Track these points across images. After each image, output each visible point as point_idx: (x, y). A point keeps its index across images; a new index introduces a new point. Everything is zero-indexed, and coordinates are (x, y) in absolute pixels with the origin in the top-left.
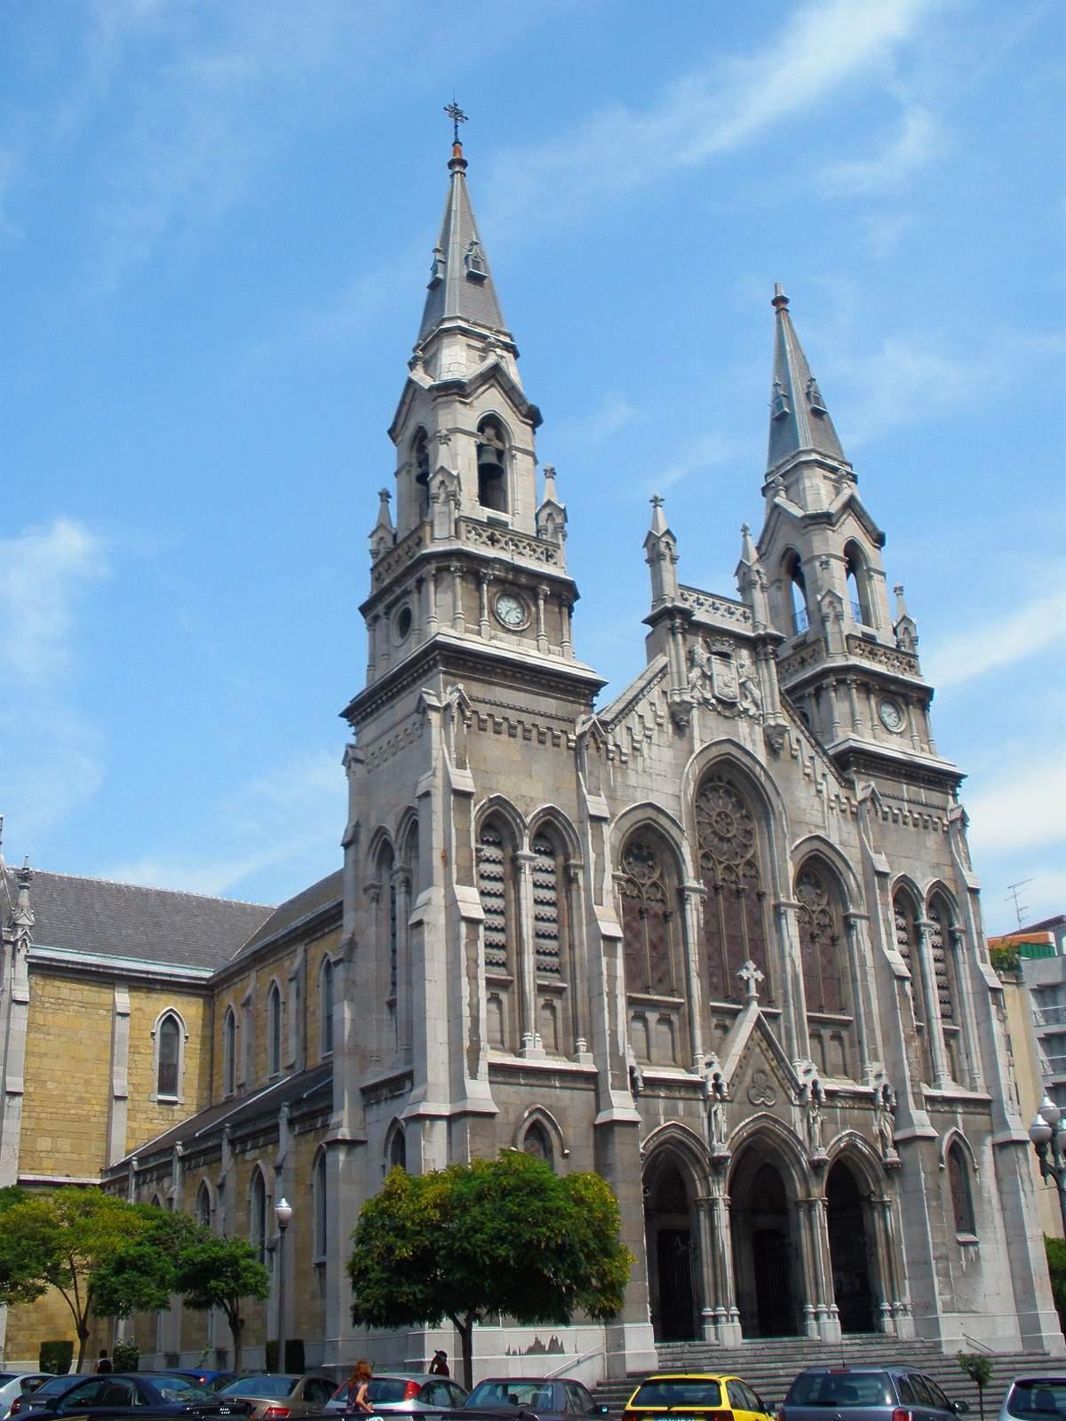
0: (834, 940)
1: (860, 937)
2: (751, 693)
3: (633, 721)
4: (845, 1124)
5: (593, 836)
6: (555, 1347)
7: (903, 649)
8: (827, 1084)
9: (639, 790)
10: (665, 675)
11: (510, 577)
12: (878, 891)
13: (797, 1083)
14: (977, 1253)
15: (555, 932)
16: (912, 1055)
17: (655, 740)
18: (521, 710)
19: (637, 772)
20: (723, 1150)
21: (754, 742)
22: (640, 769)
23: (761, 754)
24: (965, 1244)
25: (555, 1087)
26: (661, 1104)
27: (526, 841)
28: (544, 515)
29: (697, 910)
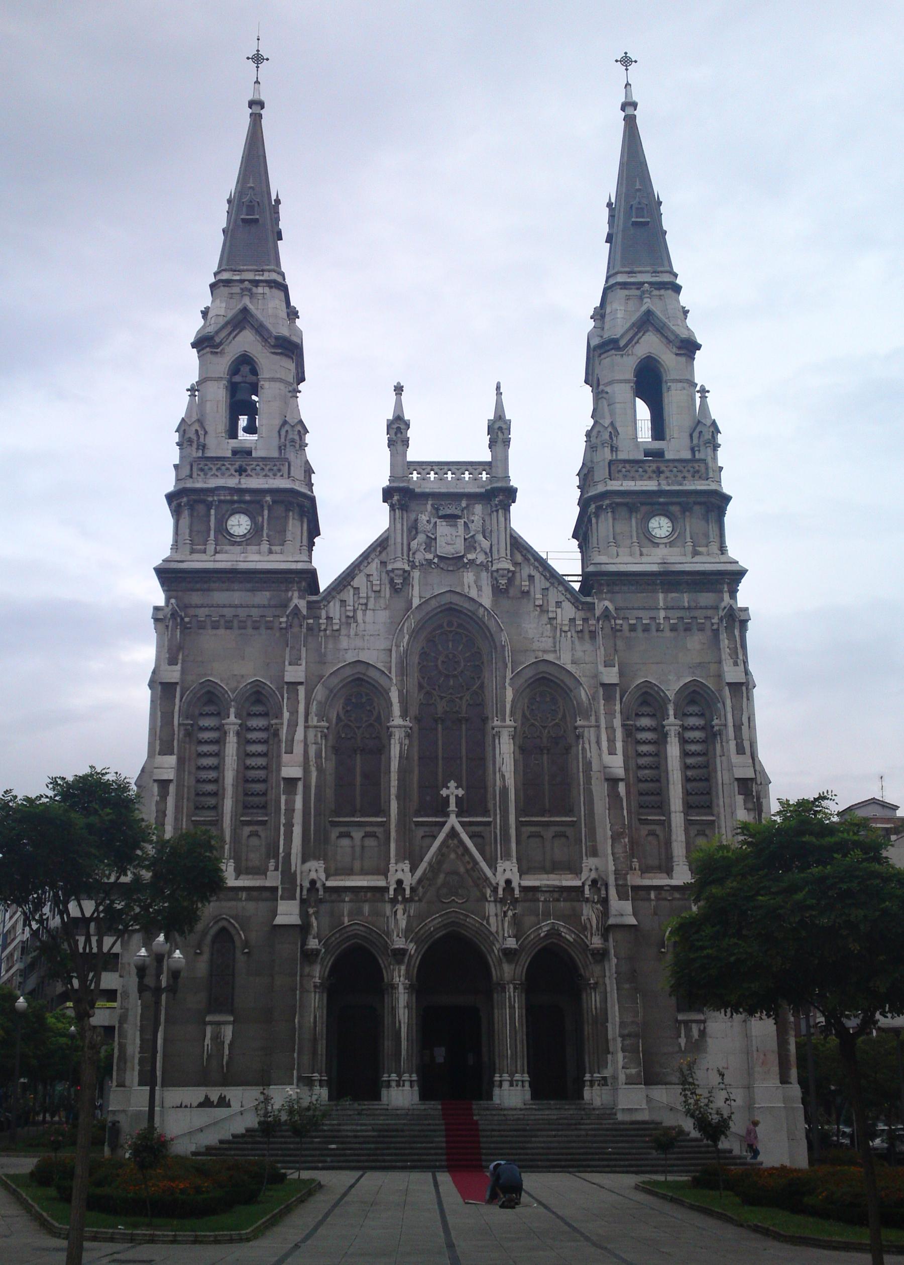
0: (568, 749)
1: (587, 746)
2: (480, 544)
3: (348, 595)
4: (547, 915)
5: (288, 698)
6: (223, 1102)
7: (697, 456)
8: (528, 882)
9: (350, 652)
10: (385, 549)
11: (235, 498)
12: (602, 702)
13: (491, 884)
14: (703, 1033)
15: (264, 777)
16: (619, 849)
17: (370, 606)
18: (236, 607)
19: (349, 636)
20: (399, 943)
21: (480, 589)
22: (352, 632)
23: (486, 600)
24: (687, 1023)
25: (241, 900)
26: (346, 908)
27: (232, 710)
28: (283, 433)
29: (401, 744)
